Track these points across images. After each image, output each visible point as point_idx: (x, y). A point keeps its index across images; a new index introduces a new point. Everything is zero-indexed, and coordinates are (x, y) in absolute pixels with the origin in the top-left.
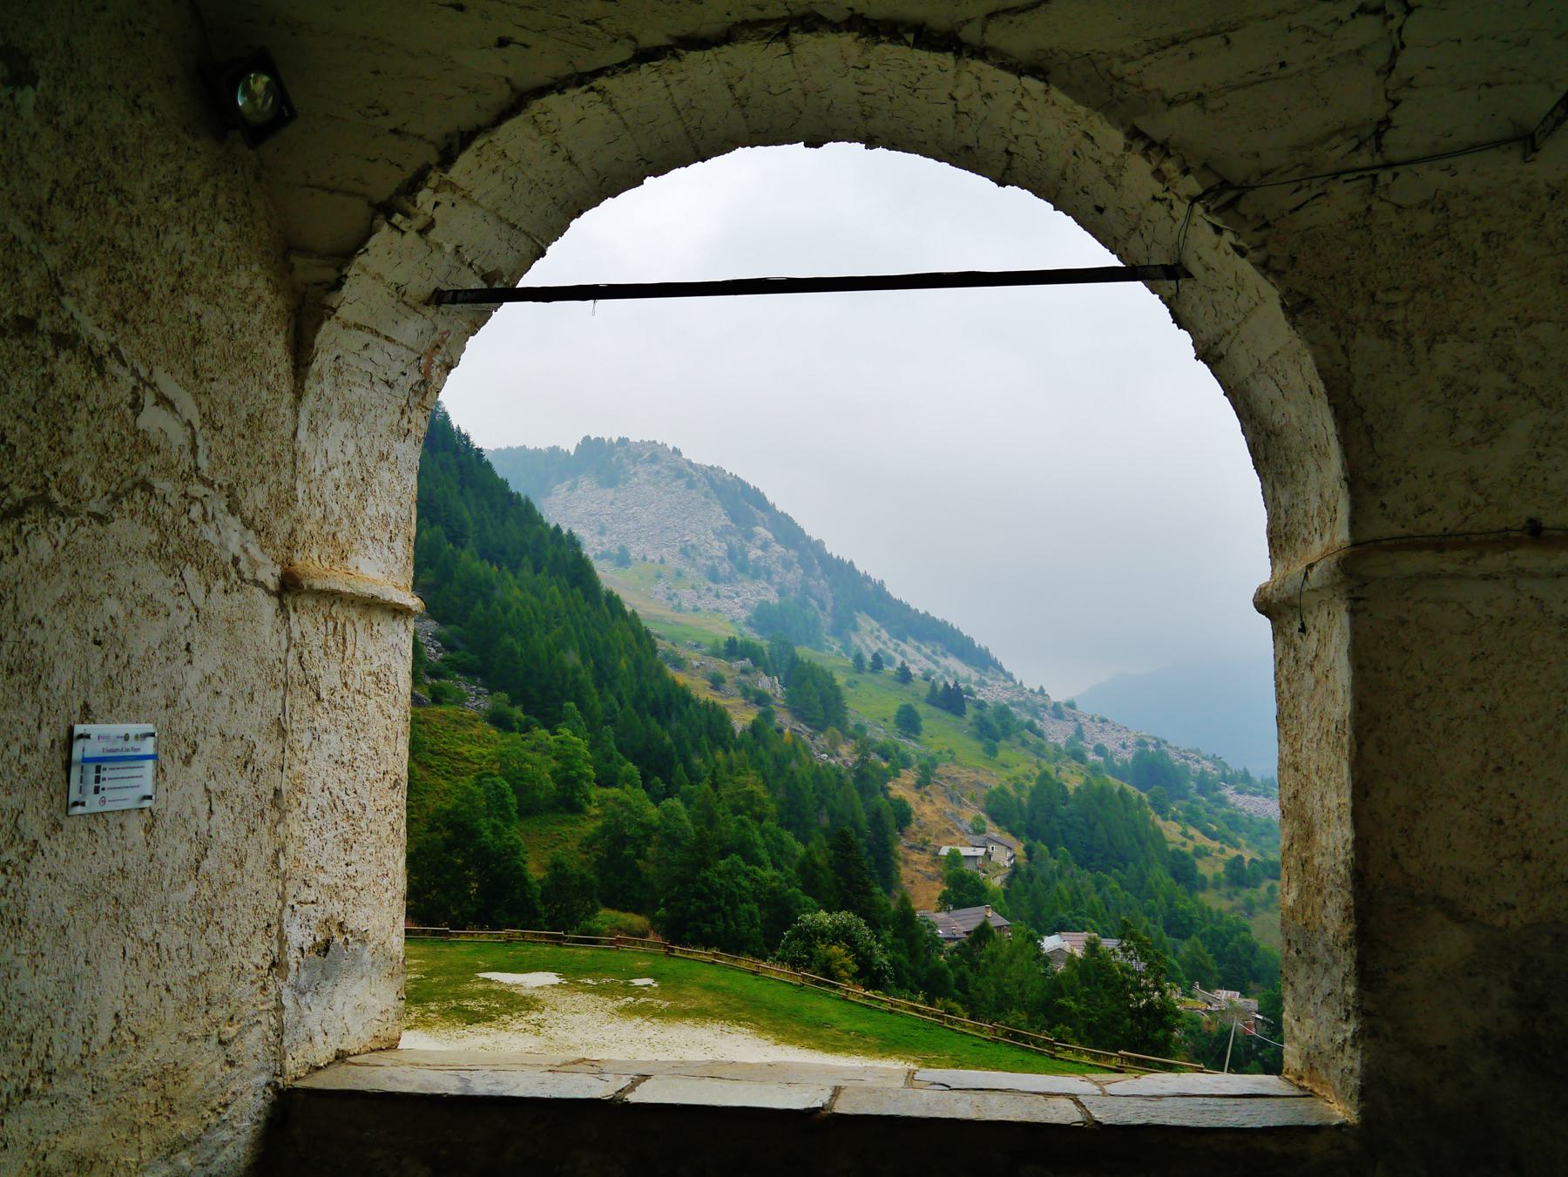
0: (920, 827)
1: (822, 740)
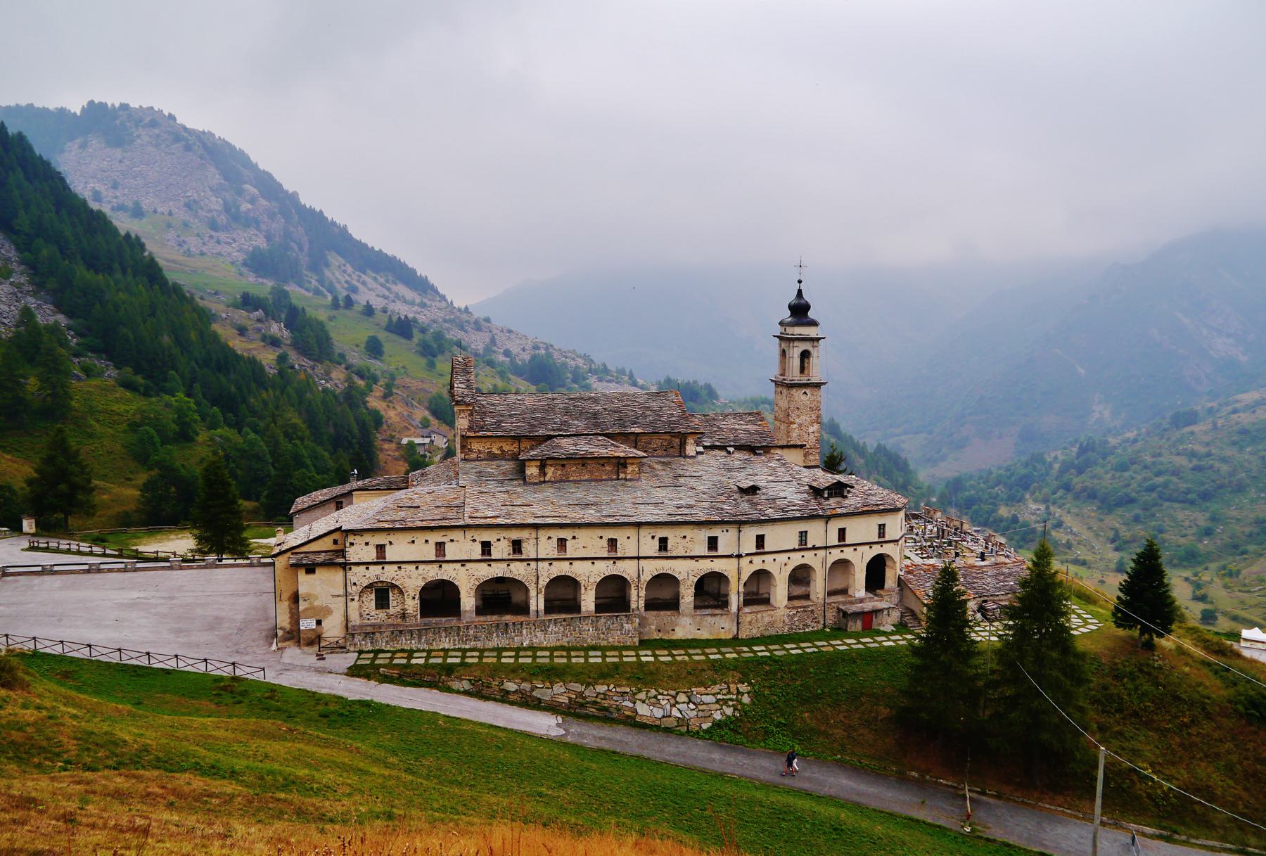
0: (388, 426)
1: (320, 369)
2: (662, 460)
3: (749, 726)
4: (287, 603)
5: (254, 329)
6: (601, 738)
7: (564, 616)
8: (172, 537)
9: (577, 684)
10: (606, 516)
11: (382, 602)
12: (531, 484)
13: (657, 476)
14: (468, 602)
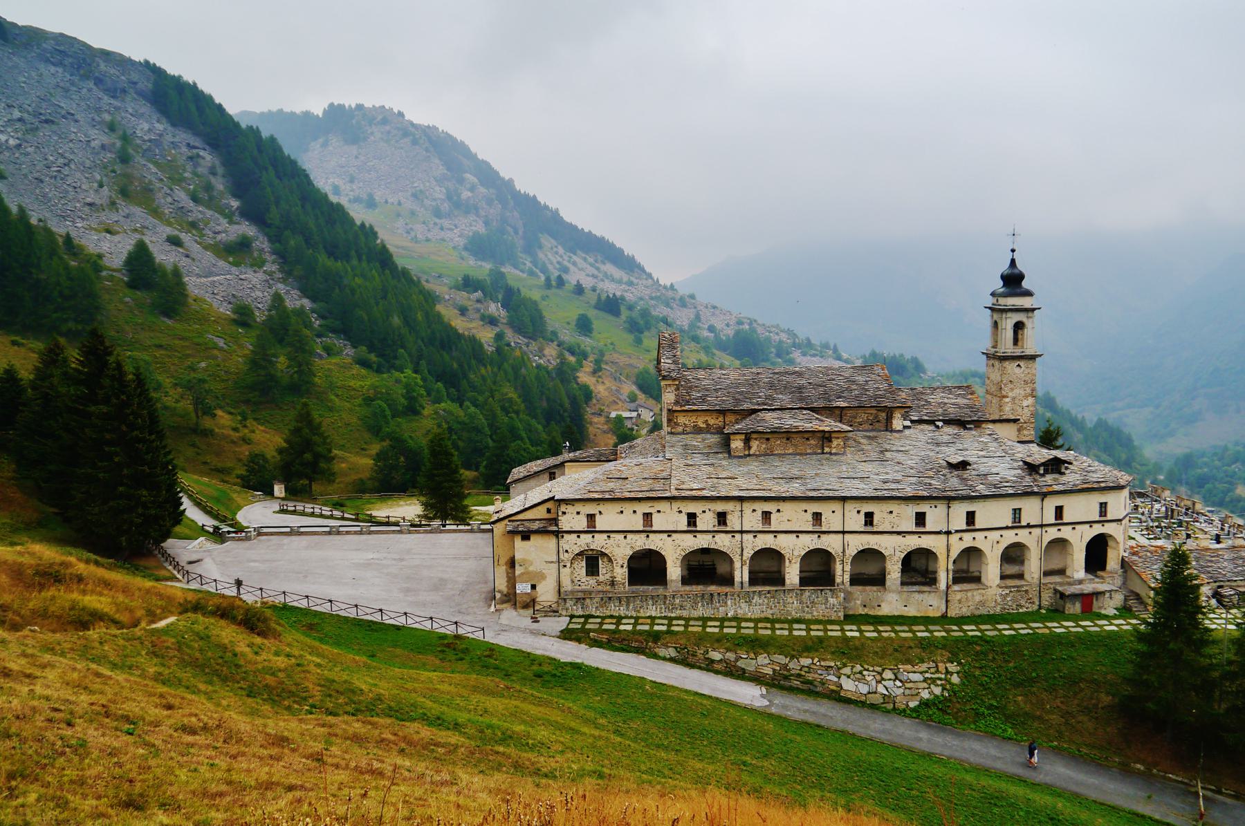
1: (534, 346)
2: (868, 434)
3: (958, 706)
4: (504, 568)
5: (474, 309)
6: (806, 711)
7: (768, 588)
8: (402, 503)
9: (781, 656)
10: (810, 490)
11: (592, 569)
12: (735, 457)
13: (862, 450)
14: (674, 571)
